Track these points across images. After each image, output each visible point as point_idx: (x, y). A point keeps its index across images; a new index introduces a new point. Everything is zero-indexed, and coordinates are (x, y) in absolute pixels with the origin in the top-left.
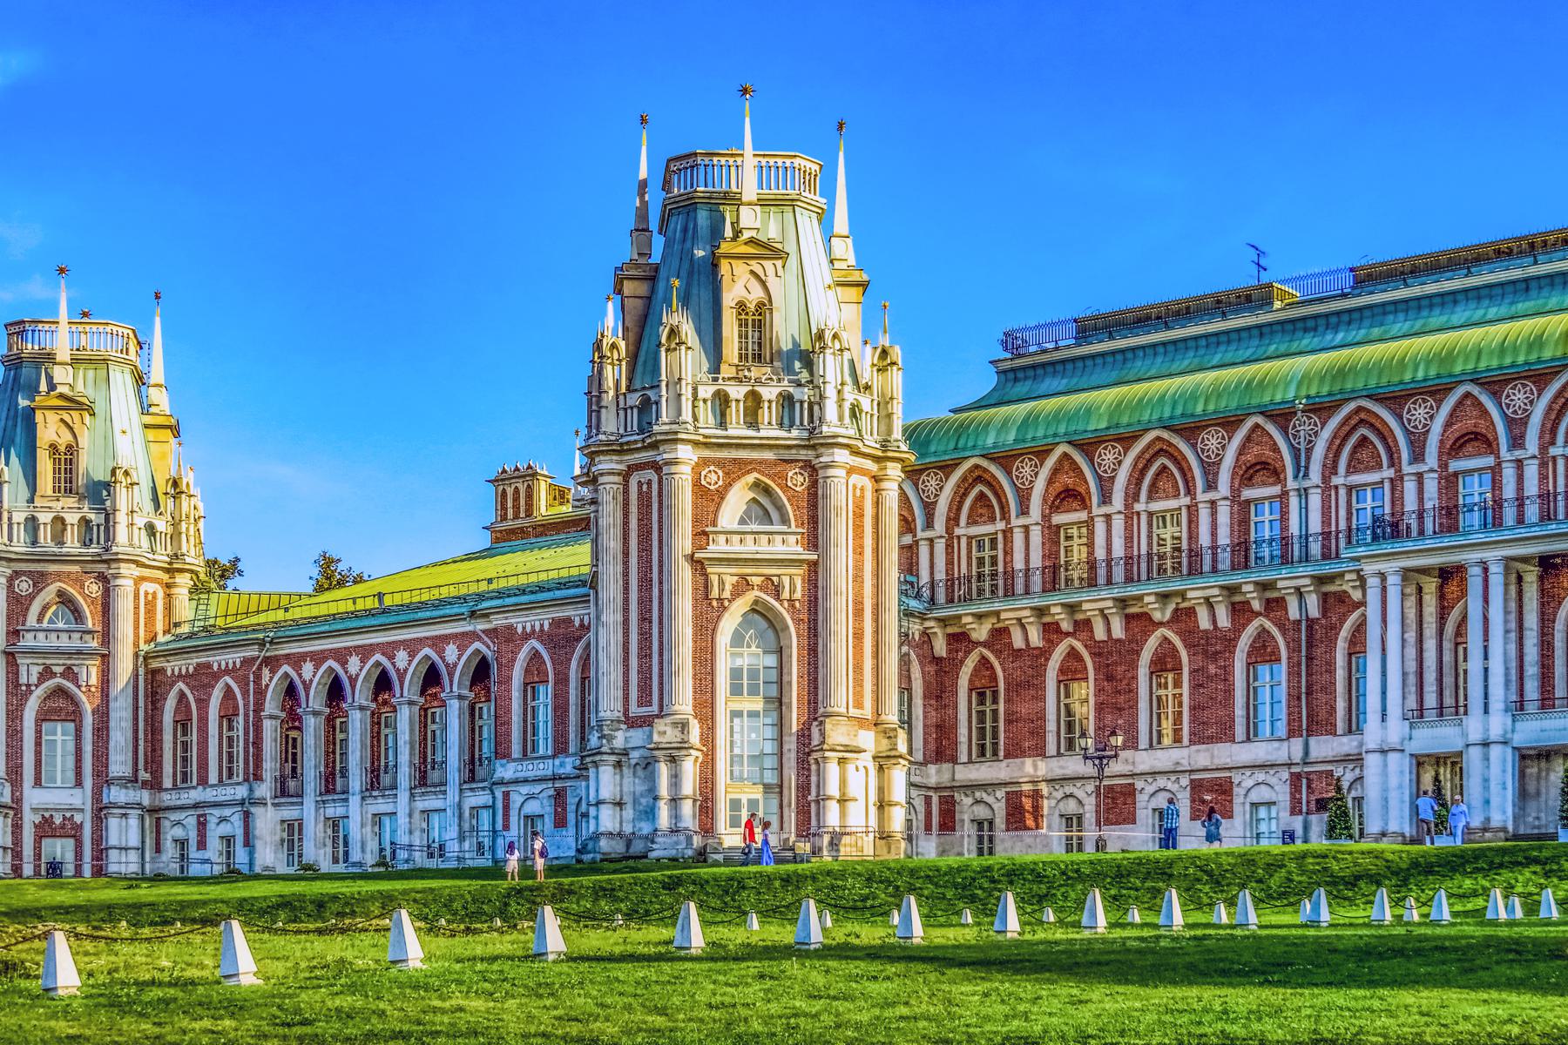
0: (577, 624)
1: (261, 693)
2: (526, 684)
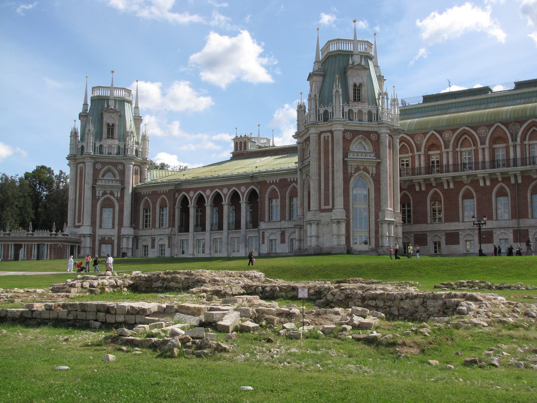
0: (289, 180)
1: (175, 200)
2: (270, 199)
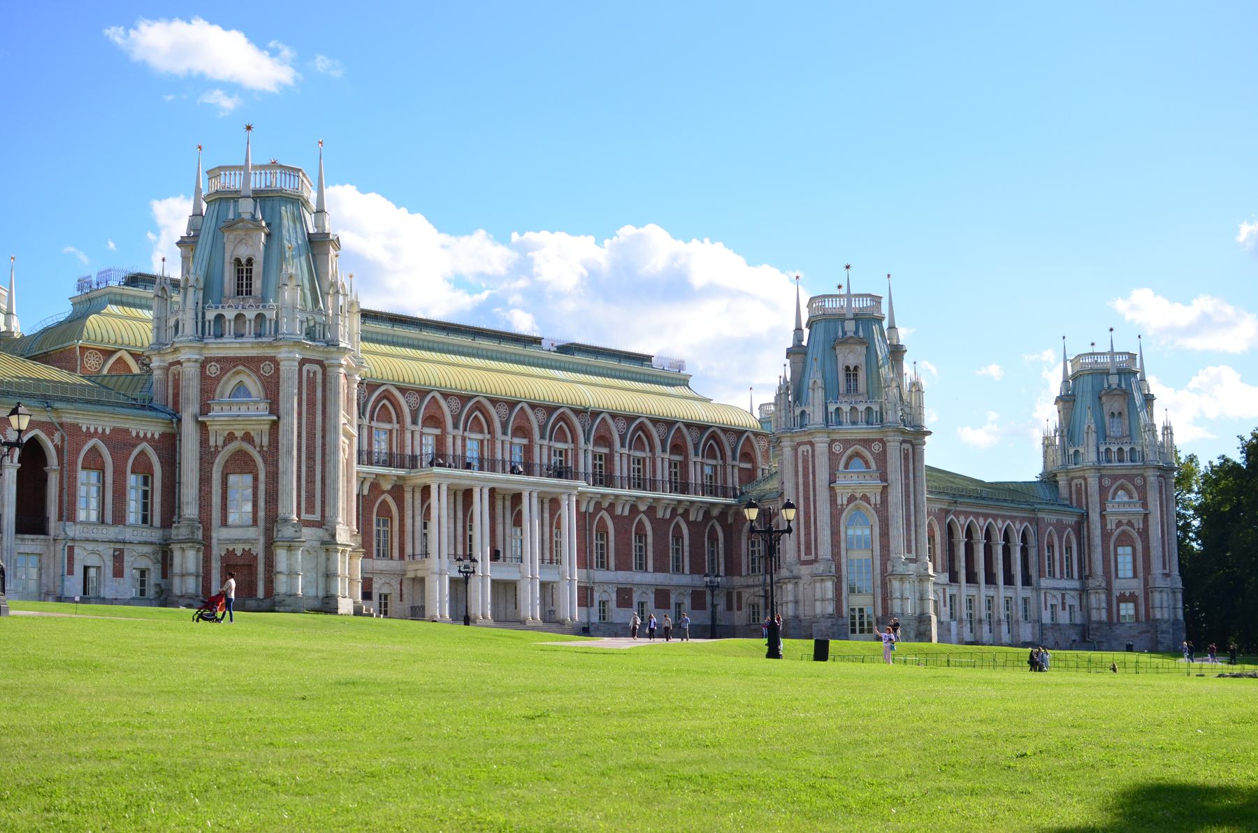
0: (134, 434)
